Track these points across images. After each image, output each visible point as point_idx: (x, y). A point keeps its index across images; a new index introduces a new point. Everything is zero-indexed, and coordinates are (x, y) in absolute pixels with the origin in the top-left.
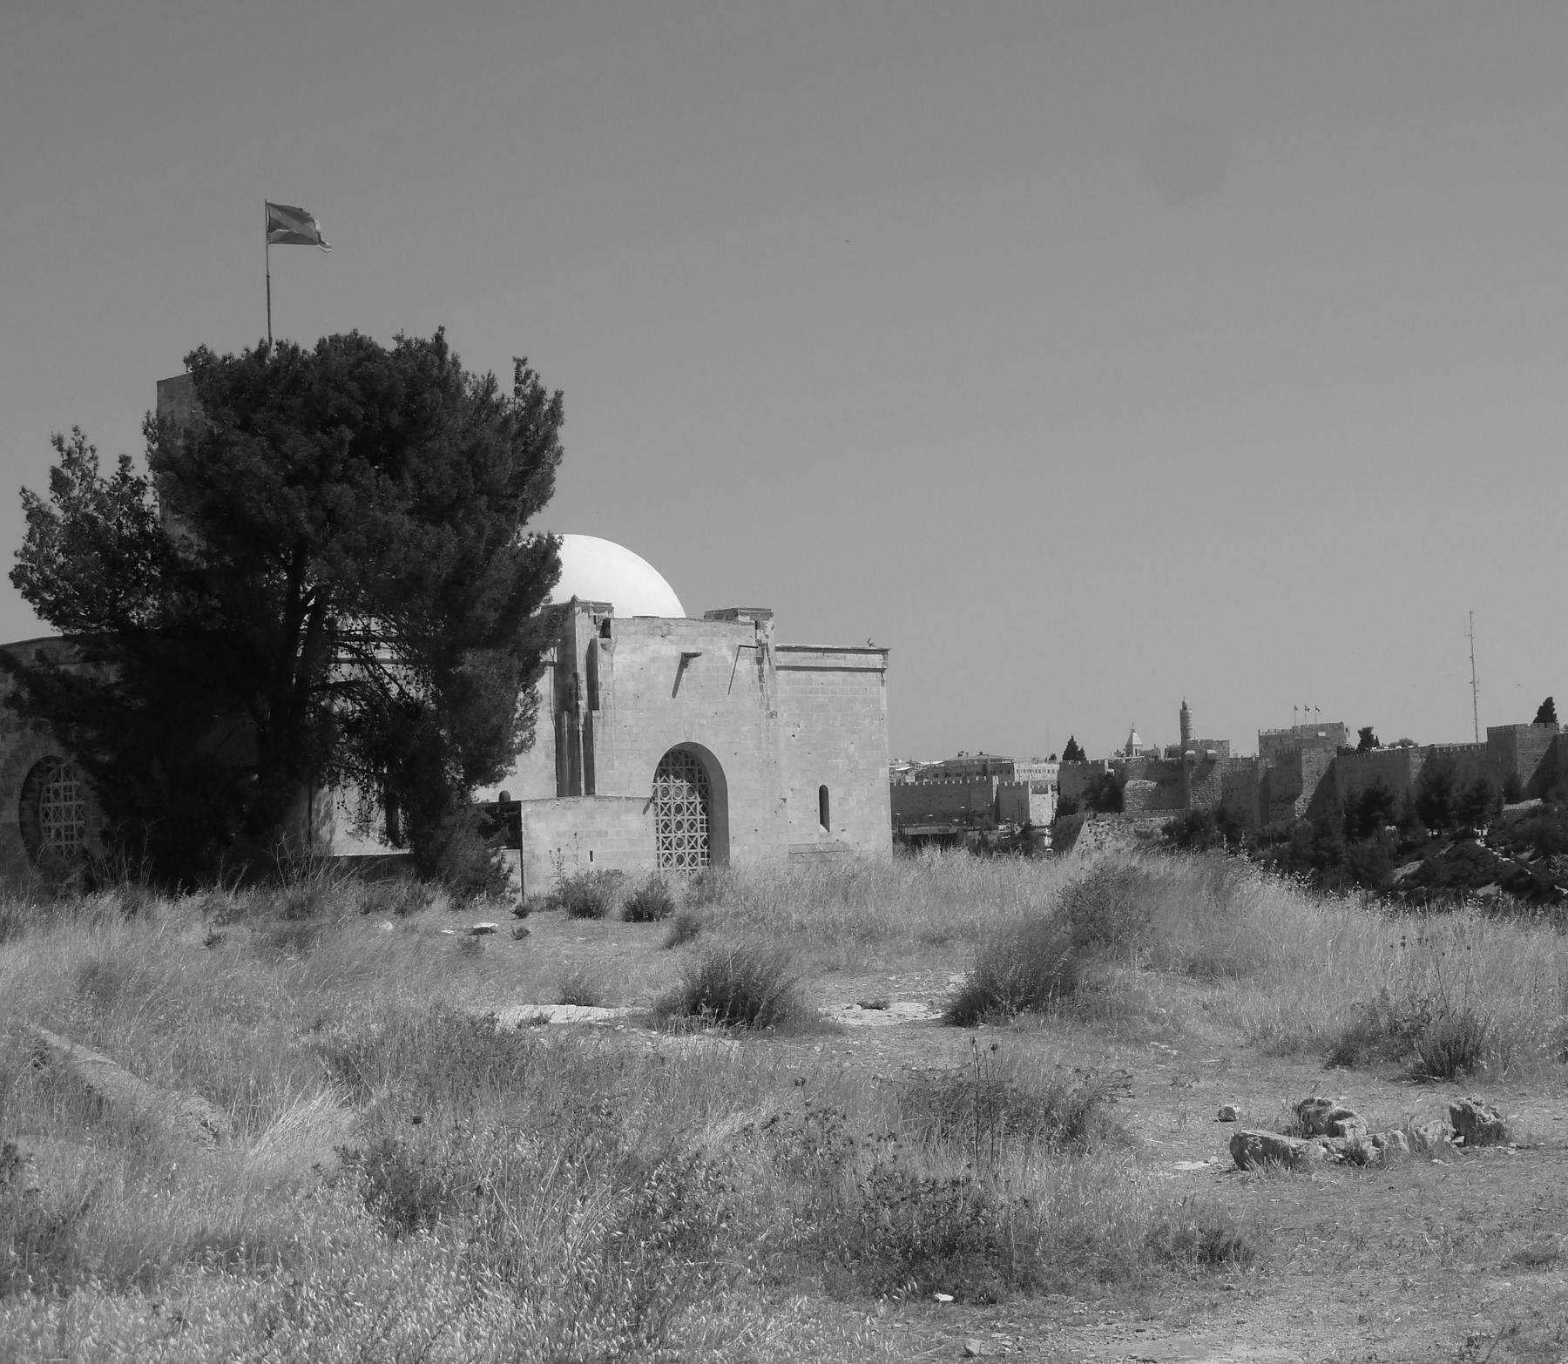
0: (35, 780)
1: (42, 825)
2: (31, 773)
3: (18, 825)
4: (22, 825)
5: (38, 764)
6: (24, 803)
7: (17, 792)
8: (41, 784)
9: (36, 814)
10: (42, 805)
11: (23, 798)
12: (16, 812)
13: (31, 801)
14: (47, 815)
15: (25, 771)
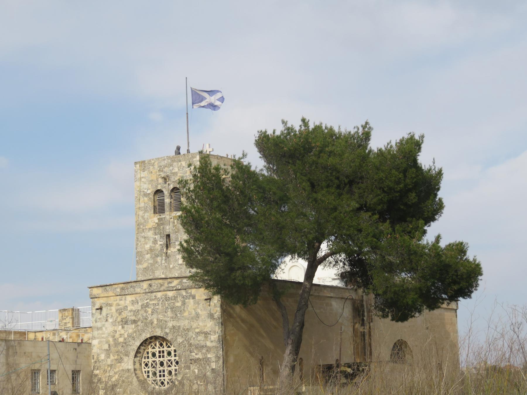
0: (142, 348)
1: (143, 370)
2: (141, 345)
3: (133, 370)
4: (135, 370)
5: (146, 340)
6: (135, 359)
7: (133, 354)
8: (144, 350)
9: (141, 364)
10: (143, 360)
11: (136, 356)
12: (131, 362)
13: (138, 358)
14: (146, 365)
15: (138, 344)
